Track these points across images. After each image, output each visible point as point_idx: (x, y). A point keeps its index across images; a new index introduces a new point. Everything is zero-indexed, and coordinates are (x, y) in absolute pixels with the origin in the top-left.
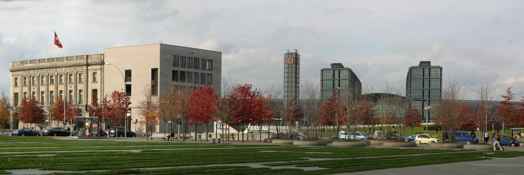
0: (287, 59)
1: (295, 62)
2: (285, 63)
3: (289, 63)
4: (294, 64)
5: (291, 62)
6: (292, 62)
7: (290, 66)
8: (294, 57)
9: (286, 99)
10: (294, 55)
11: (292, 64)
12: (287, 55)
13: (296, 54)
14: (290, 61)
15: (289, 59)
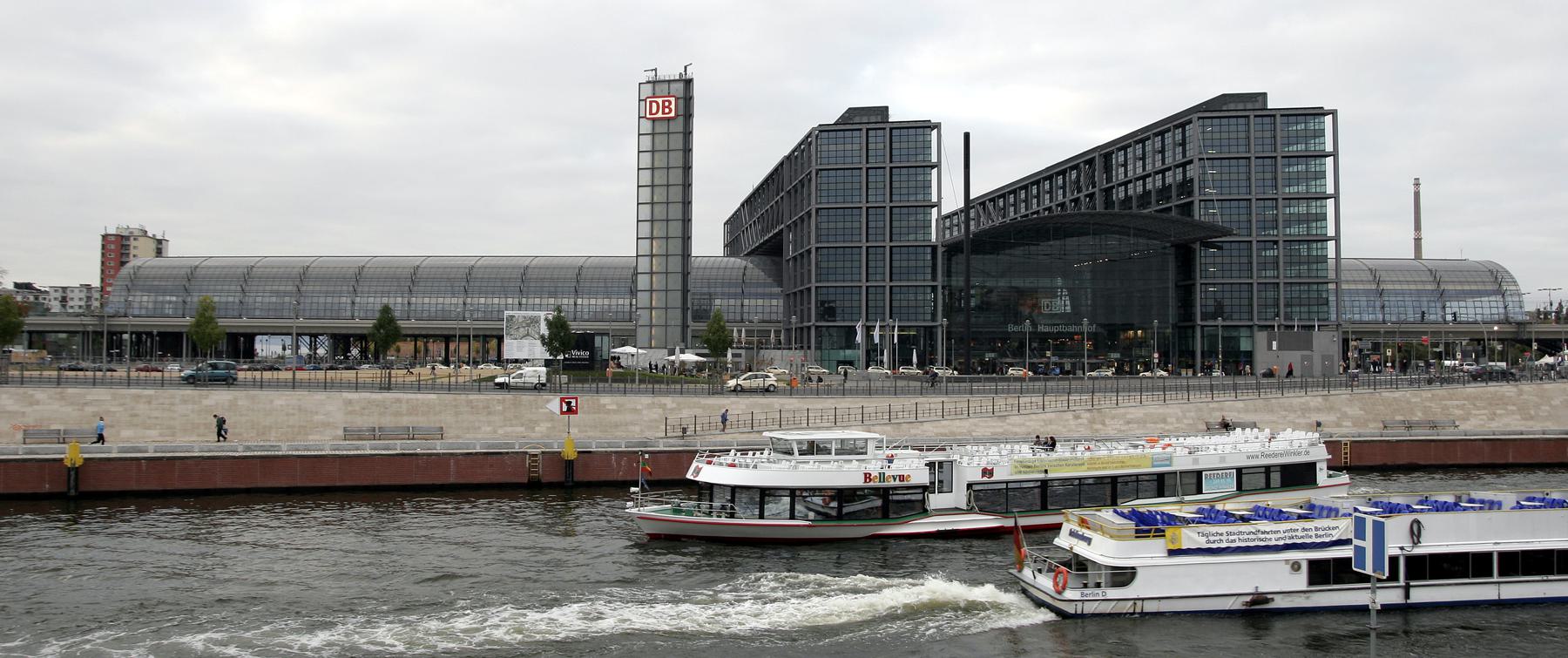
0: (651, 102)
1: (681, 112)
2: (642, 114)
3: (660, 115)
4: (681, 119)
5: (667, 110)
6: (670, 111)
7: (661, 128)
8: (681, 94)
9: (645, 245)
10: (681, 86)
11: (669, 119)
12: (650, 86)
13: (688, 83)
14: (668, 107)
15: (660, 100)
